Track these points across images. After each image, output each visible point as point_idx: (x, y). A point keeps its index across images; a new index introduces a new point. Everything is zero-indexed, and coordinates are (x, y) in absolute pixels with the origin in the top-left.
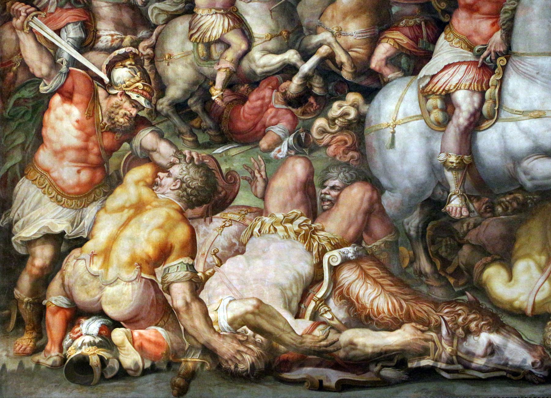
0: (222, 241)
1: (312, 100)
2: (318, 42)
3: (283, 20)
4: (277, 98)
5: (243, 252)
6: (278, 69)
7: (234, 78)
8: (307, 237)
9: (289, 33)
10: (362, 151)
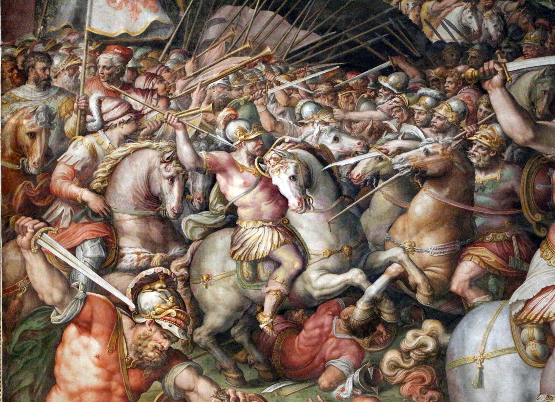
1: (380, 328)
2: (386, 260)
3: (344, 234)
4: (338, 325)
6: (339, 291)
7: (287, 302)
9: (351, 249)
10: (444, 390)
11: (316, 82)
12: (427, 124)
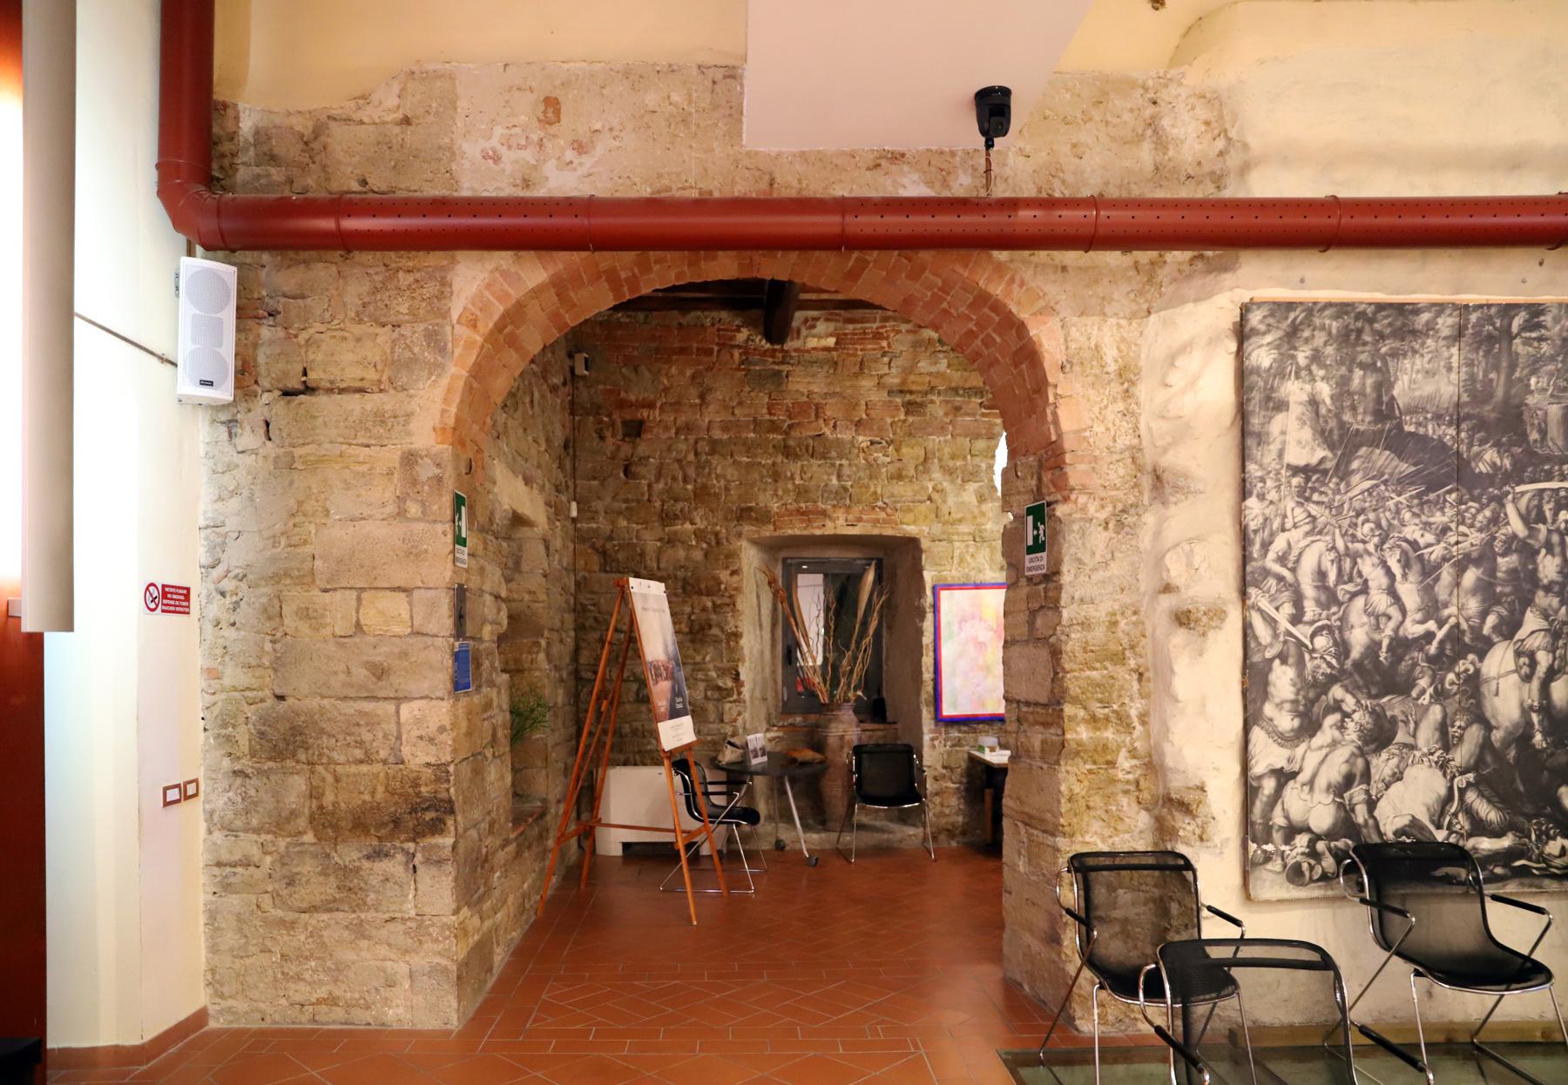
0: (1387, 772)
5: (1400, 779)
11: (1412, 497)
12: (1472, 526)
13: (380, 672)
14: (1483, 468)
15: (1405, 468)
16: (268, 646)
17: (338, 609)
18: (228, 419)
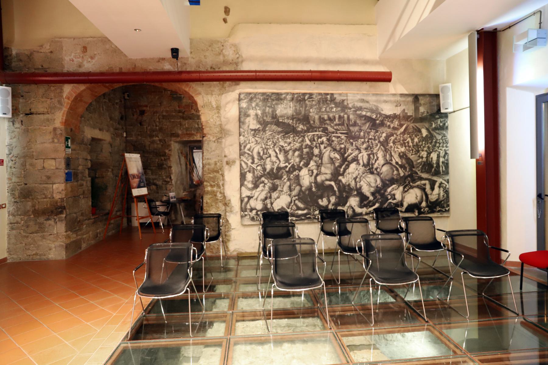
8: (290, 195)
13: (49, 177)
14: (299, 129)
15: (280, 129)
16: (23, 172)
17: (39, 163)
18: (12, 121)
